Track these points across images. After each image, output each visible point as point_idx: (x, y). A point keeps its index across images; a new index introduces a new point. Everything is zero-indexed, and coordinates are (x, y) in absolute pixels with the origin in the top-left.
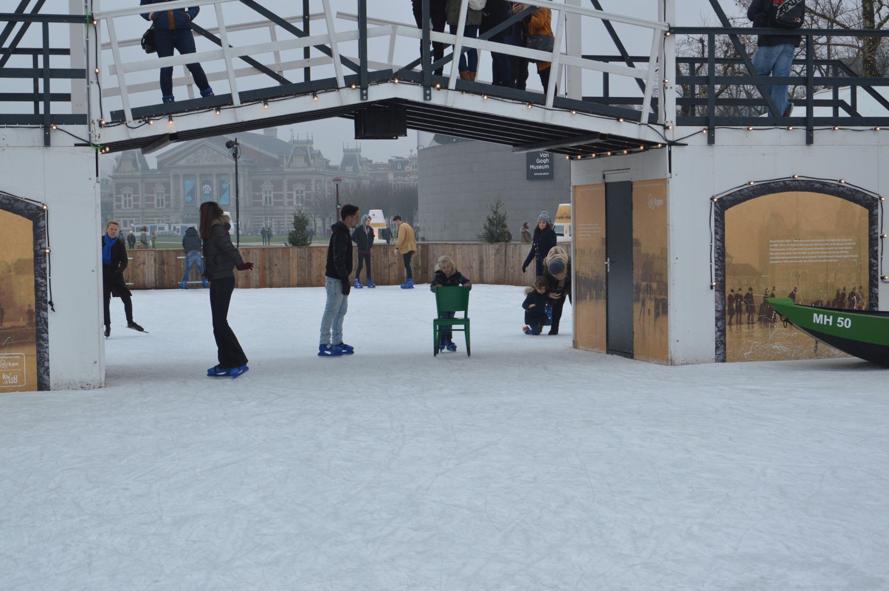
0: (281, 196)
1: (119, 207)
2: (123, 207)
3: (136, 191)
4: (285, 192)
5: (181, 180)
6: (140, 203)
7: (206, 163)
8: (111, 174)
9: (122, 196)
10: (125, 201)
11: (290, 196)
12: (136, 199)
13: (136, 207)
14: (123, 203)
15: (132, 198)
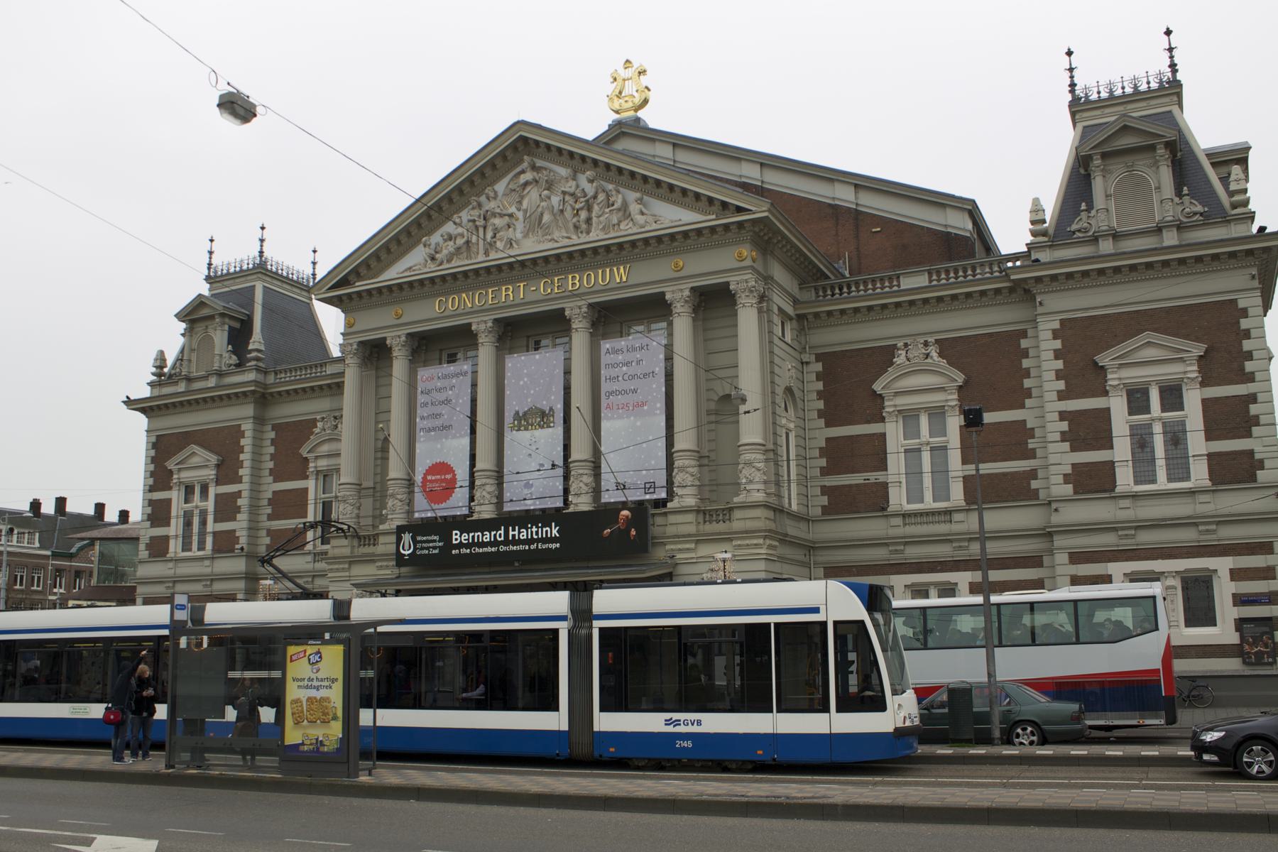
0: (1017, 441)
1: (158, 548)
2: (175, 547)
3: (227, 471)
4: (1046, 407)
5: (399, 366)
6: (240, 525)
7: (531, 246)
8: (146, 392)
9: (175, 496)
10: (188, 524)
11: (1089, 430)
12: (226, 508)
13: (225, 544)
14: (175, 528)
15: (210, 505)
